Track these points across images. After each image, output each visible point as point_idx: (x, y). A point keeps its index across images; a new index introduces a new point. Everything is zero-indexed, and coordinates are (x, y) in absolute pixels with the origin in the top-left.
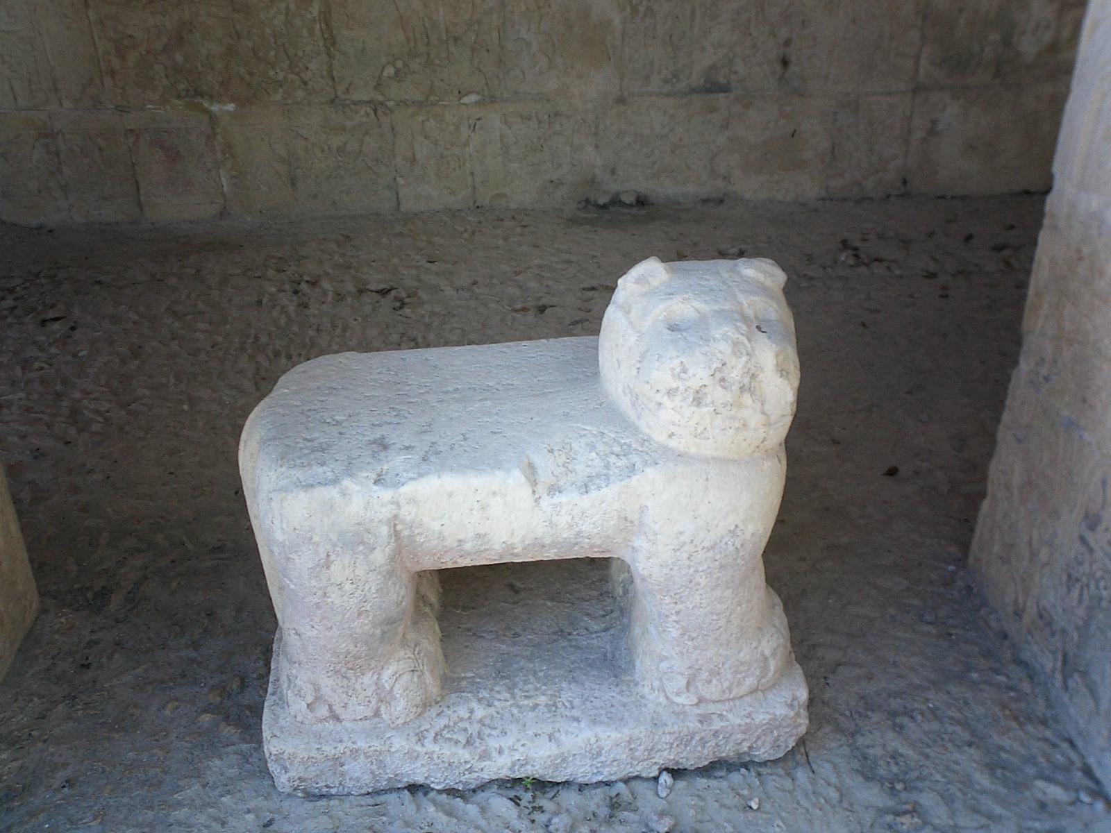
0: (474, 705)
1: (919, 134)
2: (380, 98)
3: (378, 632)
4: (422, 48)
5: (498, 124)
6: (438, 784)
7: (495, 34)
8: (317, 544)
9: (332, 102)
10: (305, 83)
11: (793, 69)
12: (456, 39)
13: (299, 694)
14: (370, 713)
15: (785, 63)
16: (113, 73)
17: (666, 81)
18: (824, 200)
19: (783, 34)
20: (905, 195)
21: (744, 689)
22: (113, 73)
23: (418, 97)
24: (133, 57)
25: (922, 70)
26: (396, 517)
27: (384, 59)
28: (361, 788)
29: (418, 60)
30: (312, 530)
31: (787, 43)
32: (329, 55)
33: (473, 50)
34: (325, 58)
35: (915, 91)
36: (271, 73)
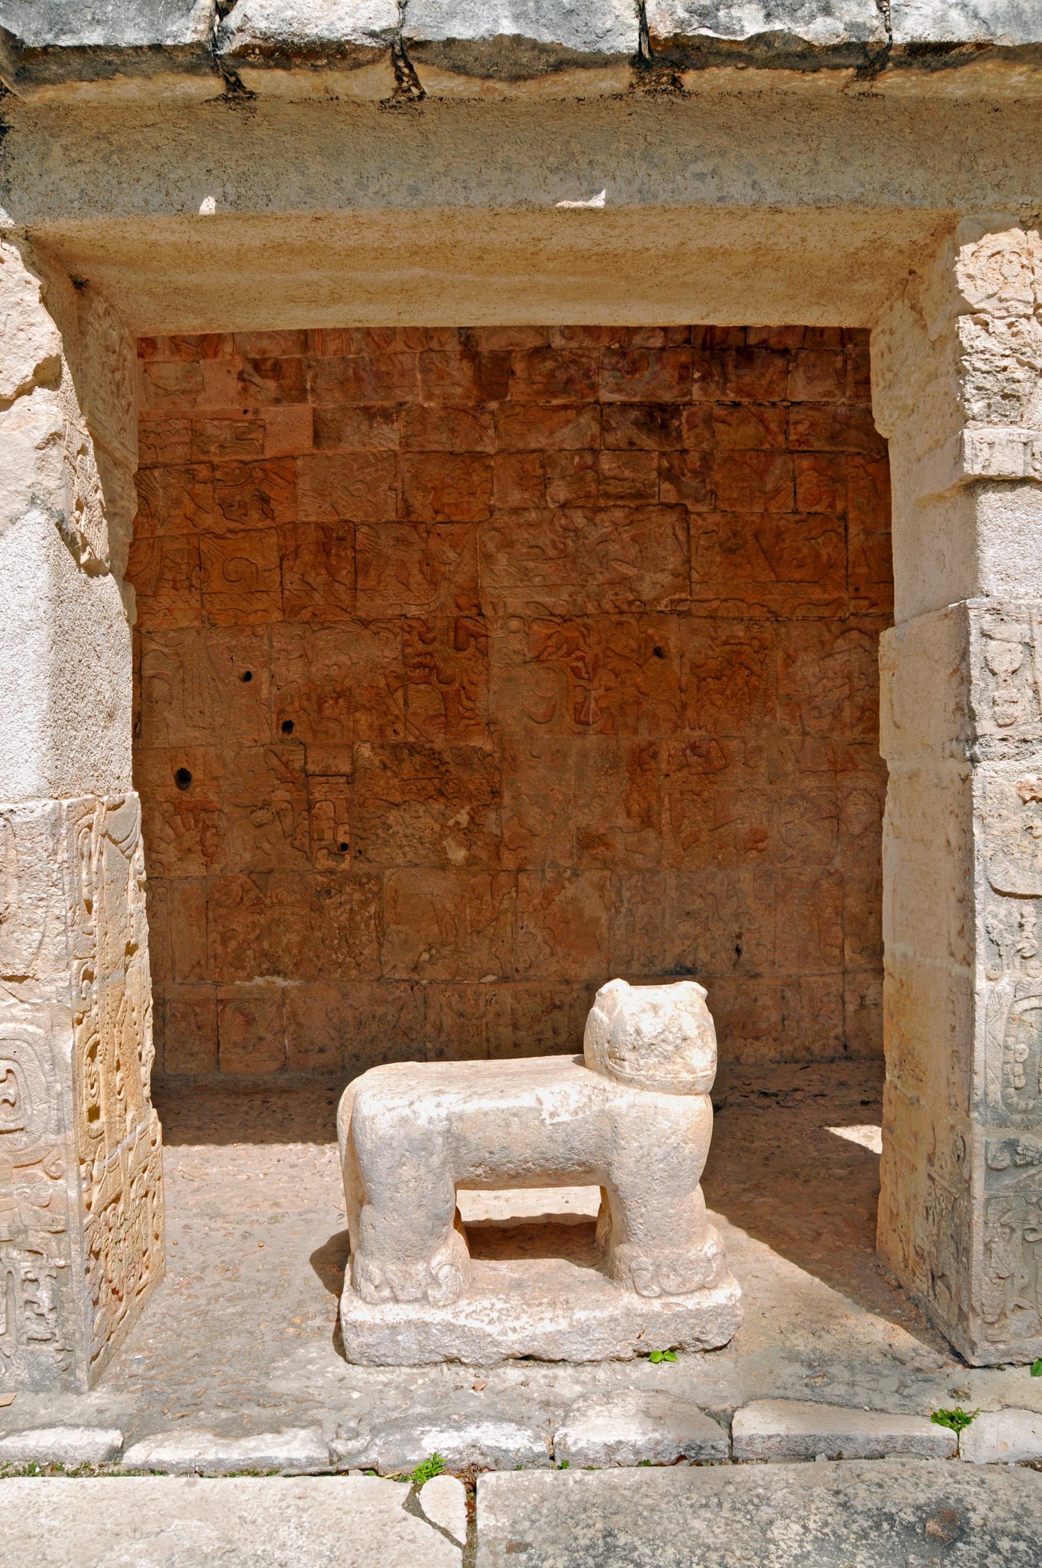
0: (494, 1300)
1: (851, 1008)
2: (416, 977)
3: (430, 1225)
4: (452, 939)
5: (509, 1000)
6: (467, 1357)
7: (509, 928)
8: (394, 1149)
9: (379, 979)
10: (359, 965)
11: (745, 956)
12: (478, 933)
13: (370, 1280)
14: (419, 1295)
15: (738, 951)
16: (215, 957)
17: (644, 966)
18: (778, 1062)
19: (735, 928)
20: (848, 1058)
21: (693, 1286)
22: (215, 957)
23: (445, 976)
24: (233, 944)
25: (847, 957)
26: (448, 1131)
27: (421, 947)
28: (409, 1358)
29: (448, 948)
30: (392, 1138)
31: (739, 936)
32: (381, 945)
33: (491, 941)
34: (376, 946)
35: (844, 973)
36: (334, 956)
